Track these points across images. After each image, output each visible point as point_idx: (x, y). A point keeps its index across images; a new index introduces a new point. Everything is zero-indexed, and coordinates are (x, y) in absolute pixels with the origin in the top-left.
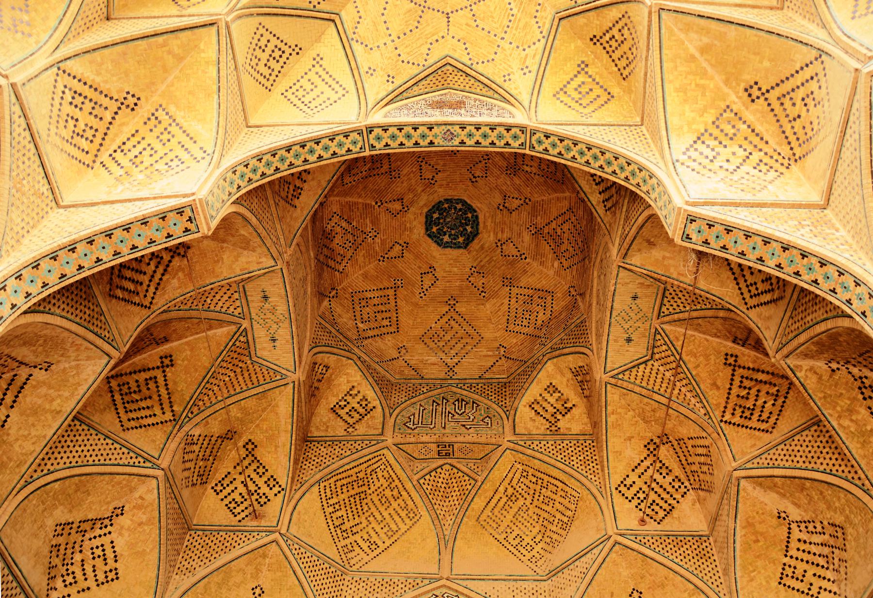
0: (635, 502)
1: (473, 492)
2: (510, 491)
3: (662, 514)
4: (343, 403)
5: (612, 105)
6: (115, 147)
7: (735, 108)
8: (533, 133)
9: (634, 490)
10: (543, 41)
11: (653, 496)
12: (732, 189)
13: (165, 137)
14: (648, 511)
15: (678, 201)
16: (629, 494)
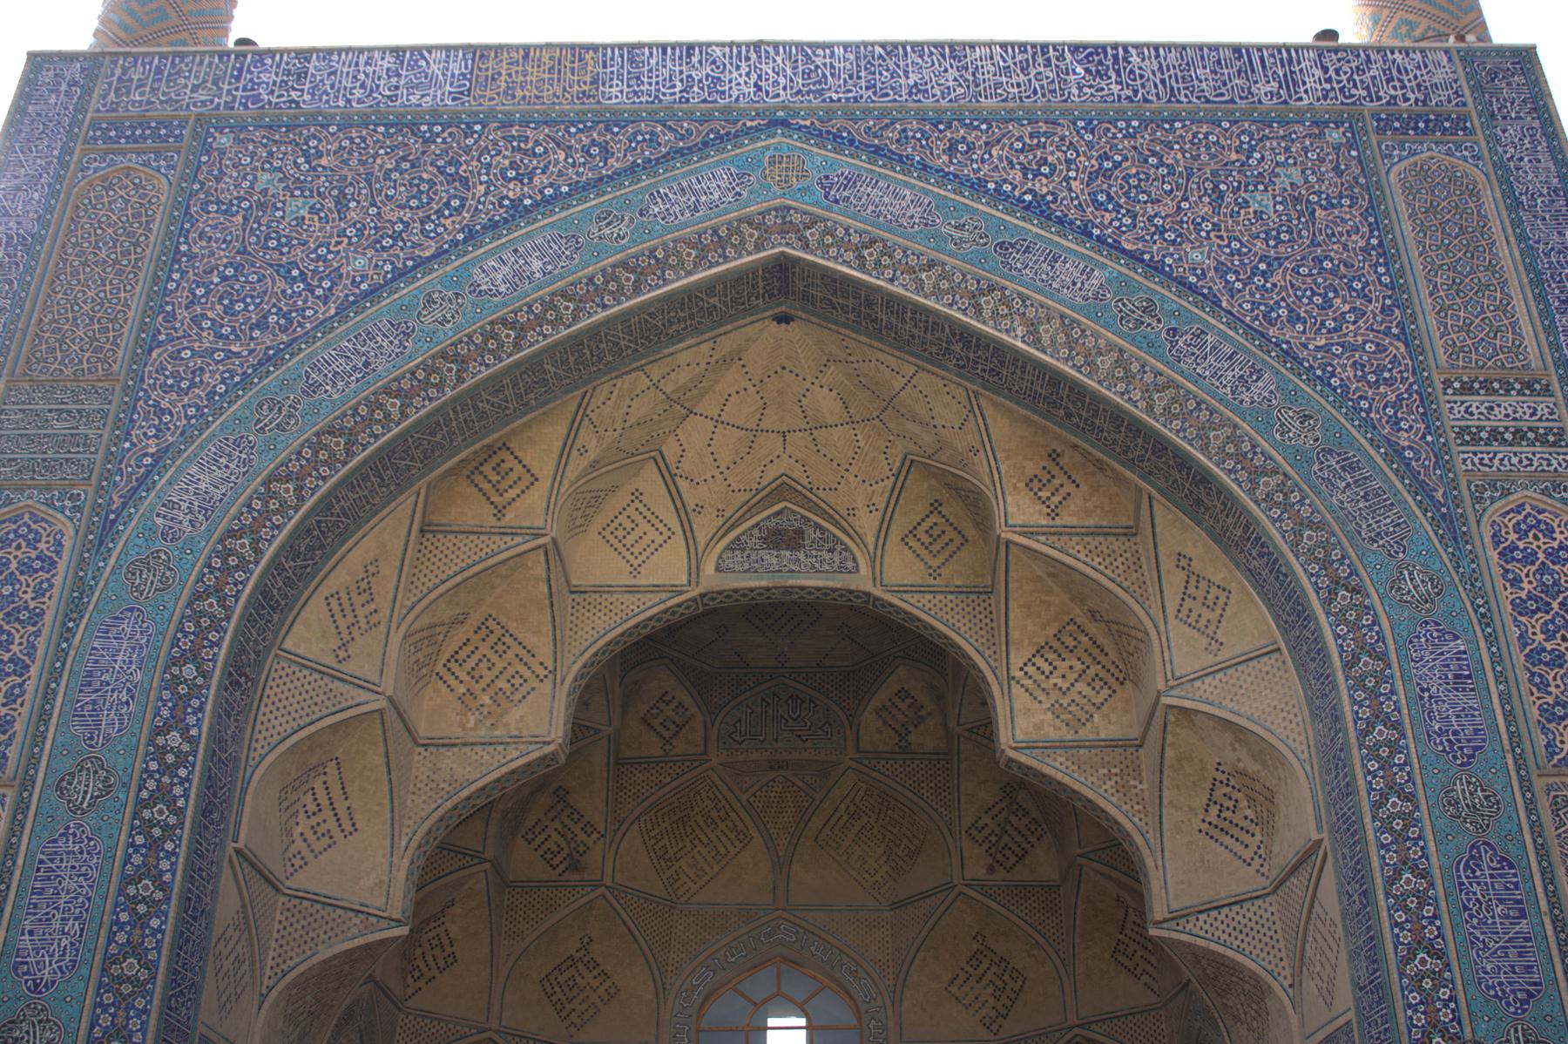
0: (986, 846)
1: (810, 811)
2: (852, 809)
3: (1013, 859)
4: (655, 711)
5: (965, 554)
6: (447, 656)
7: (1078, 620)
8: (877, 599)
9: (986, 832)
10: (892, 479)
11: (1005, 839)
12: (1058, 721)
13: (500, 648)
14: (999, 857)
15: (1003, 739)
16: (980, 837)
